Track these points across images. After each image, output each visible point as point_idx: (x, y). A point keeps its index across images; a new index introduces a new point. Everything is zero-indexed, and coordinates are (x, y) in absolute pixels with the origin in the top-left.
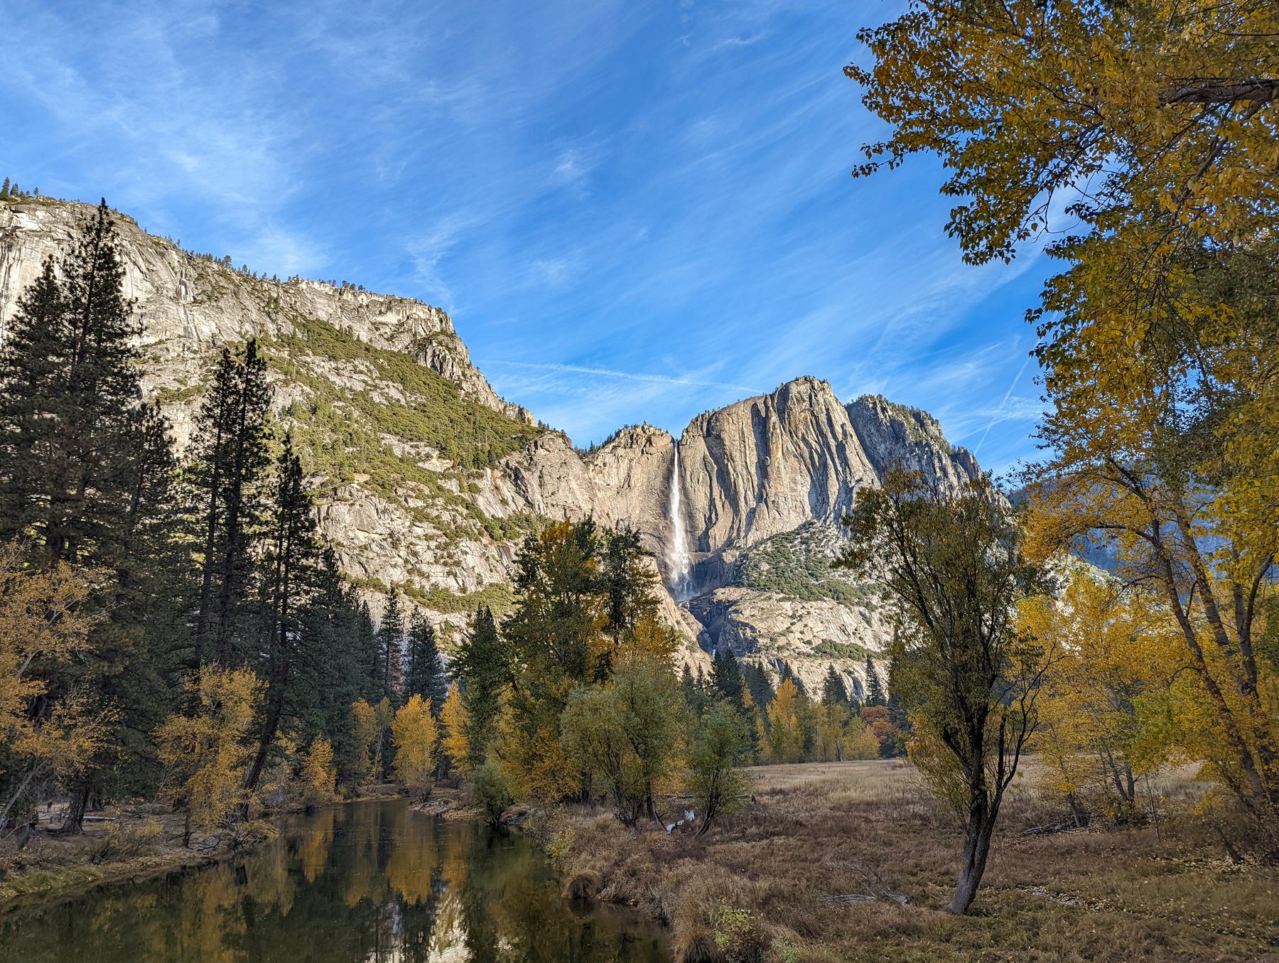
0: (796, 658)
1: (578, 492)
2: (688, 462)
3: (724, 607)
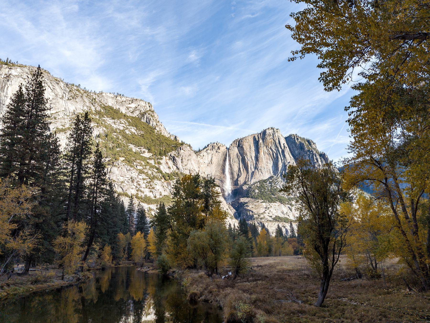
0: (267, 222)
2: (232, 156)
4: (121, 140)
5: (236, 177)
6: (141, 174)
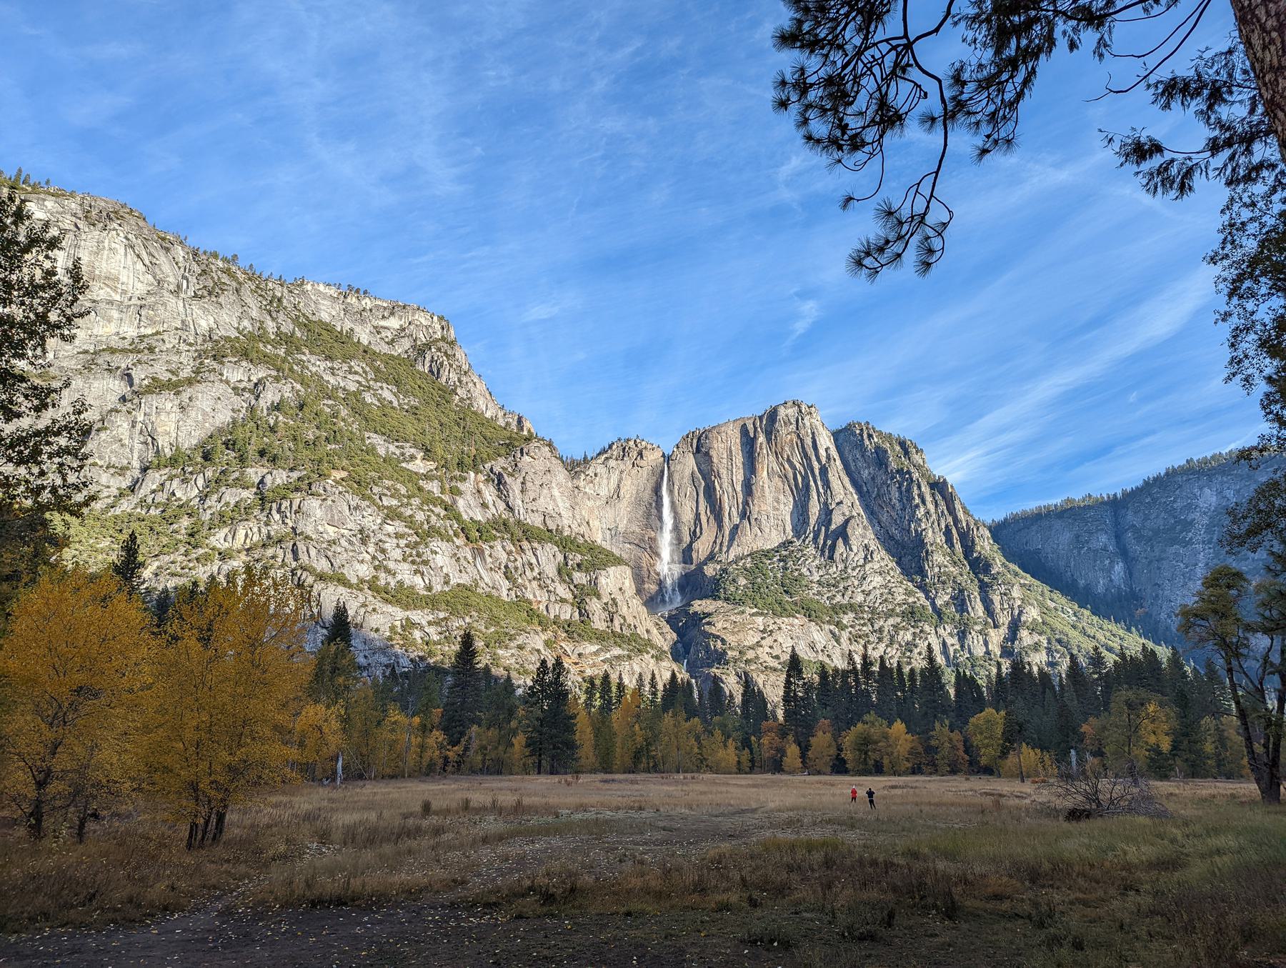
0: (762, 672)
1: (559, 501)
2: (676, 477)
3: (697, 619)
4: (343, 420)
5: (687, 539)
6: (392, 520)
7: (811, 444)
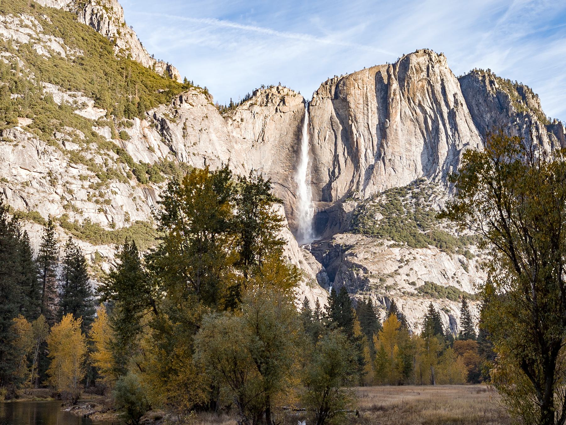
0: (401, 297)
2: (316, 121)
3: (341, 251)
4: (21, 71)
5: (326, 179)
6: (76, 163)
7: (440, 90)
